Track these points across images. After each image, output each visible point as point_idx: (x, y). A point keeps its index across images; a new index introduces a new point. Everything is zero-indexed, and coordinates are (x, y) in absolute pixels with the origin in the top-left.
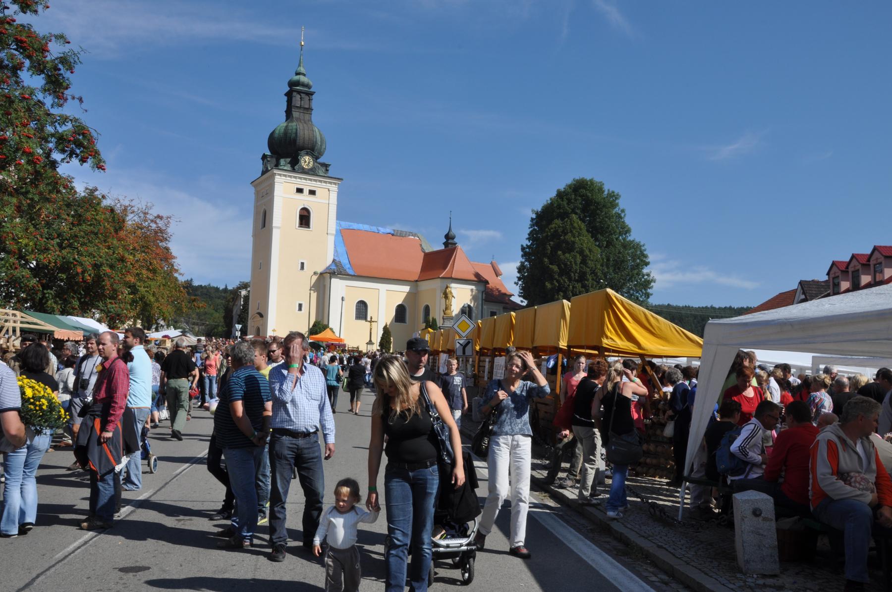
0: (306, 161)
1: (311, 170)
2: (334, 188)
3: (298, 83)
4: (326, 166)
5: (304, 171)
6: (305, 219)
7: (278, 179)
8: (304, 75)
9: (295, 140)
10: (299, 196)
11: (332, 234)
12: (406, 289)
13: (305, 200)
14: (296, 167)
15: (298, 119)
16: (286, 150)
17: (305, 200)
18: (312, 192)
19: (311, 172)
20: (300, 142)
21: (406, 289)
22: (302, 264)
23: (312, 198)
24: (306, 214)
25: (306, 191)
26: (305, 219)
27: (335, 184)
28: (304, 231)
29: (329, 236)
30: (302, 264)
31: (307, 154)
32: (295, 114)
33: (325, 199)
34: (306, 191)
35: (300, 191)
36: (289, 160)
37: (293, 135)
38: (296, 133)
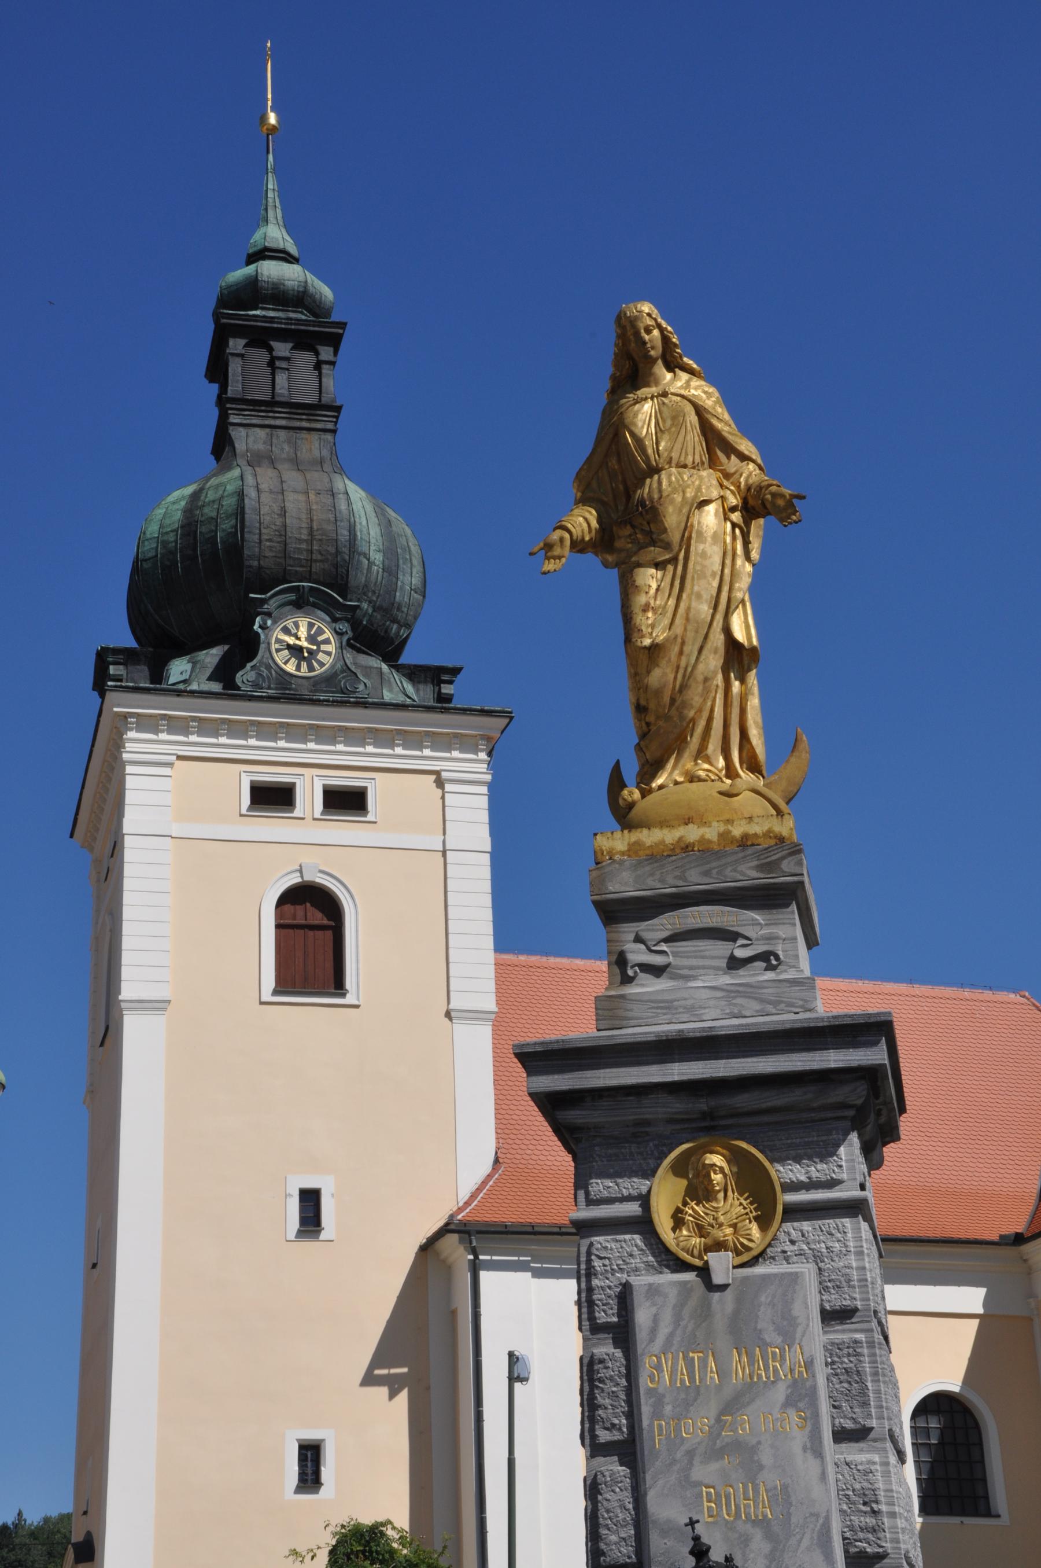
0: (298, 638)
1: (329, 680)
2: (475, 766)
3: (253, 293)
4: (434, 676)
5: (286, 692)
6: (312, 936)
7: (136, 744)
8: (286, 257)
9: (235, 547)
10: (270, 826)
11: (475, 1015)
12: (971, 1298)
13: (307, 844)
14: (244, 677)
15: (255, 460)
16: (195, 613)
17: (307, 844)
18: (345, 801)
19: (336, 691)
20: (260, 549)
21: (971, 1298)
22: (310, 1199)
23: (344, 830)
25: (309, 796)
26: (312, 936)
27: (467, 744)
28: (309, 1017)
29: (461, 1029)
30: (310, 1199)
31: (300, 603)
32: (246, 439)
33: (424, 837)
34: (309, 796)
35: (272, 797)
36: (212, 656)
37: (227, 525)
38: (240, 511)
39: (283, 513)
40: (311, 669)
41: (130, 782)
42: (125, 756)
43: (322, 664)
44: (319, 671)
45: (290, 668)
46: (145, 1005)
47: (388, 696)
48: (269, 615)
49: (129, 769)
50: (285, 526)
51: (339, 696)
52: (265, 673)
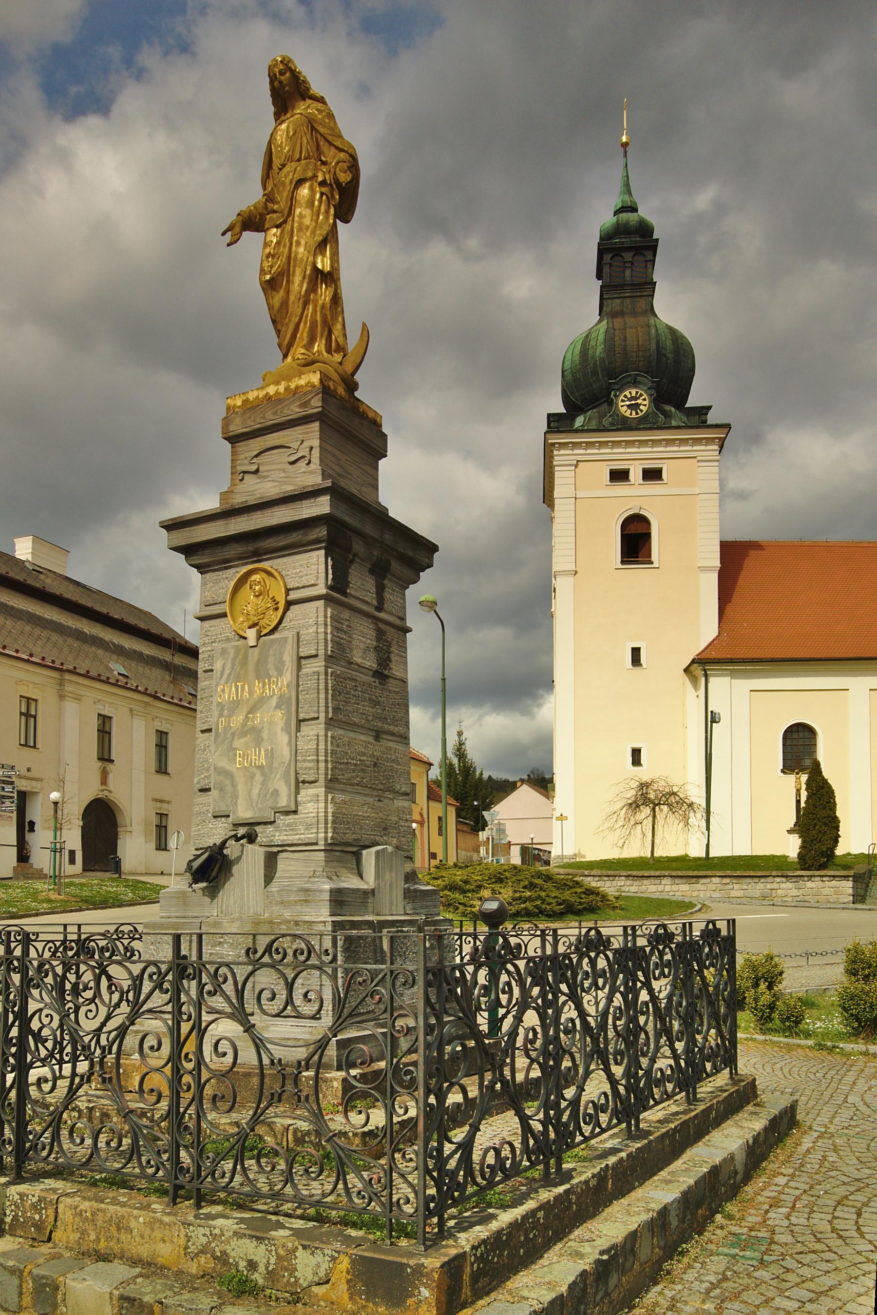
1: (645, 417)
5: (624, 425)
10: (620, 489)
13: (636, 496)
17: (636, 496)
18: (652, 475)
23: (653, 488)
24: (638, 529)
25: (636, 475)
28: (636, 573)
34: (636, 475)
35: (619, 476)
39: (625, 339)
40: (637, 413)
41: (557, 474)
42: (554, 463)
43: (642, 411)
44: (641, 414)
45: (628, 414)
46: (564, 573)
47: (674, 423)
48: (618, 390)
49: (556, 469)
50: (626, 345)
51: (649, 426)
52: (616, 418)
